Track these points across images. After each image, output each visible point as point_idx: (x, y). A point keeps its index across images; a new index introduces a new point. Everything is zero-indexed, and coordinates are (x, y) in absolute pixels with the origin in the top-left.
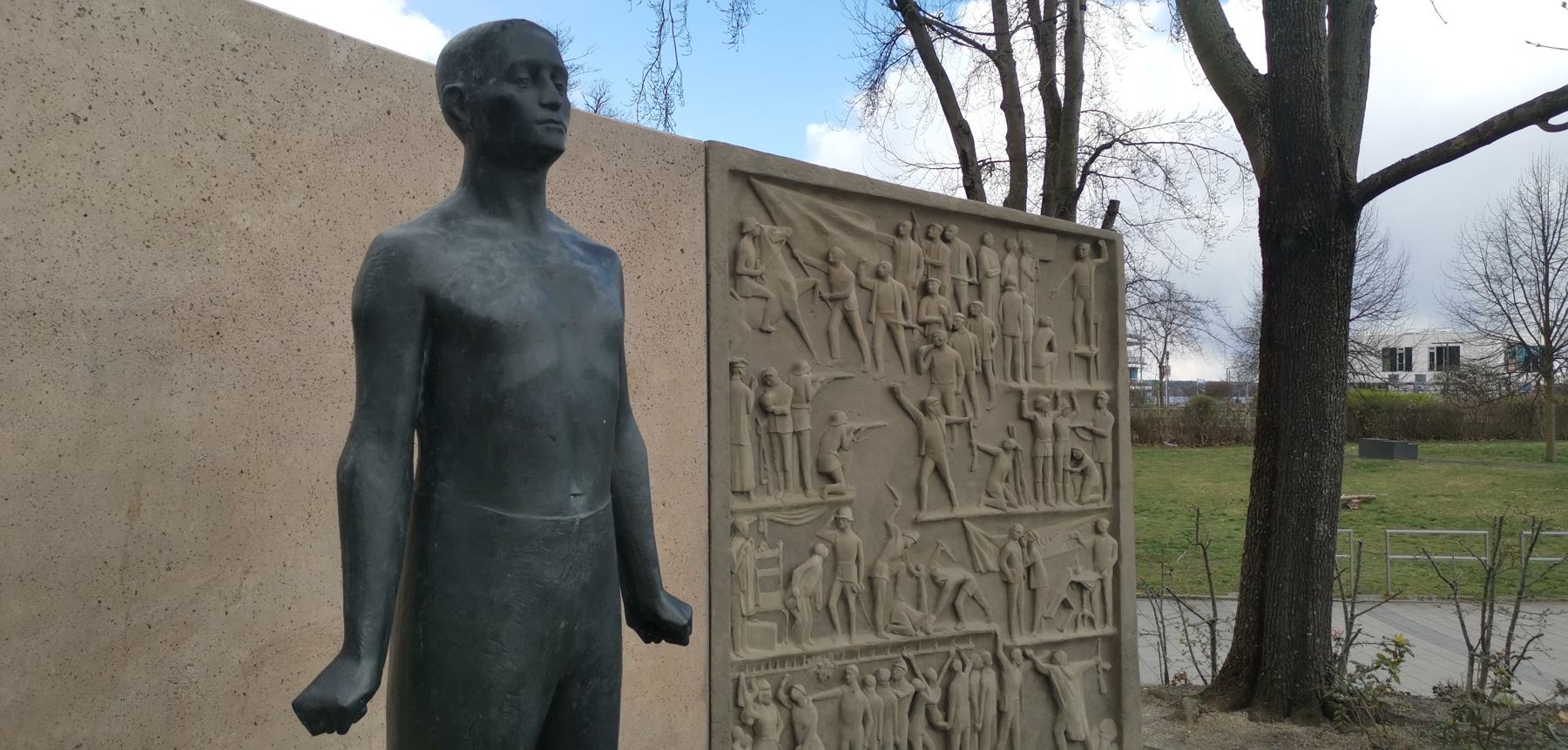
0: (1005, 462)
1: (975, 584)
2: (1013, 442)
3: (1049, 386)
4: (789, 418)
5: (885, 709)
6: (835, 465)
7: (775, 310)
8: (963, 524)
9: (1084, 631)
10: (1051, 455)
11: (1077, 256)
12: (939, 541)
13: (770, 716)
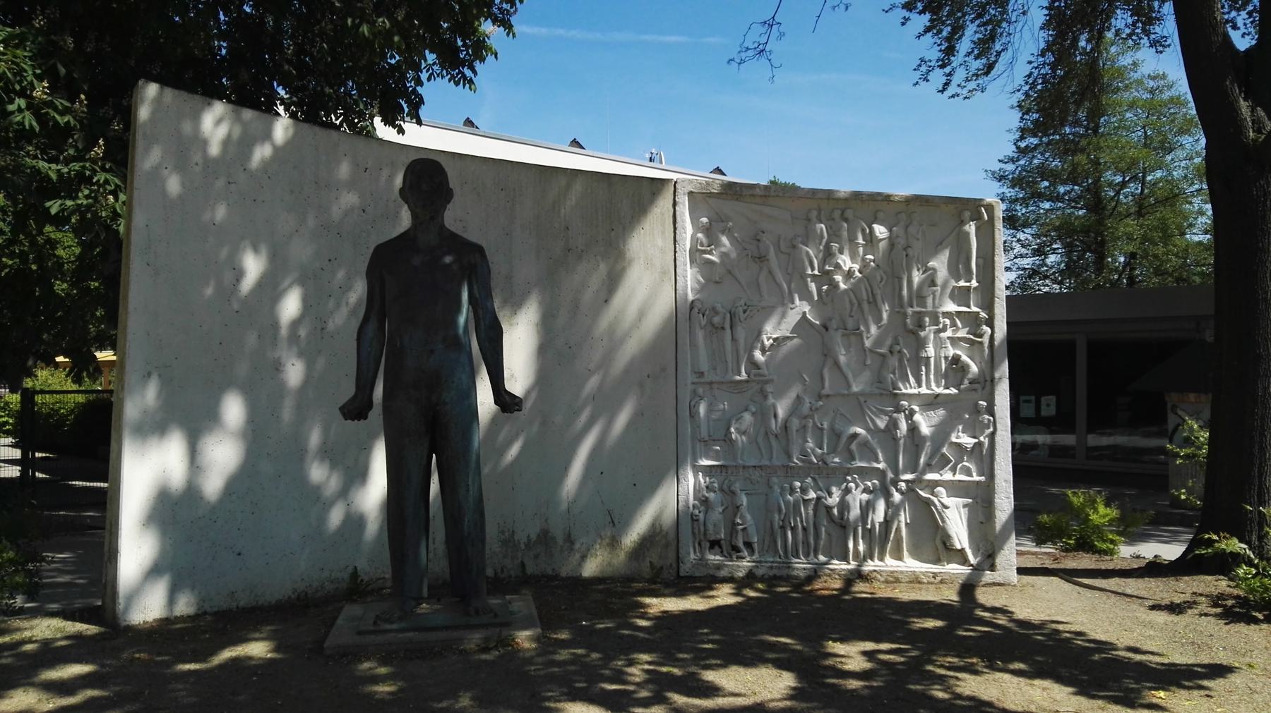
4: (728, 331)
5: (794, 505)
8: (858, 399)
10: (933, 355)
12: (840, 408)
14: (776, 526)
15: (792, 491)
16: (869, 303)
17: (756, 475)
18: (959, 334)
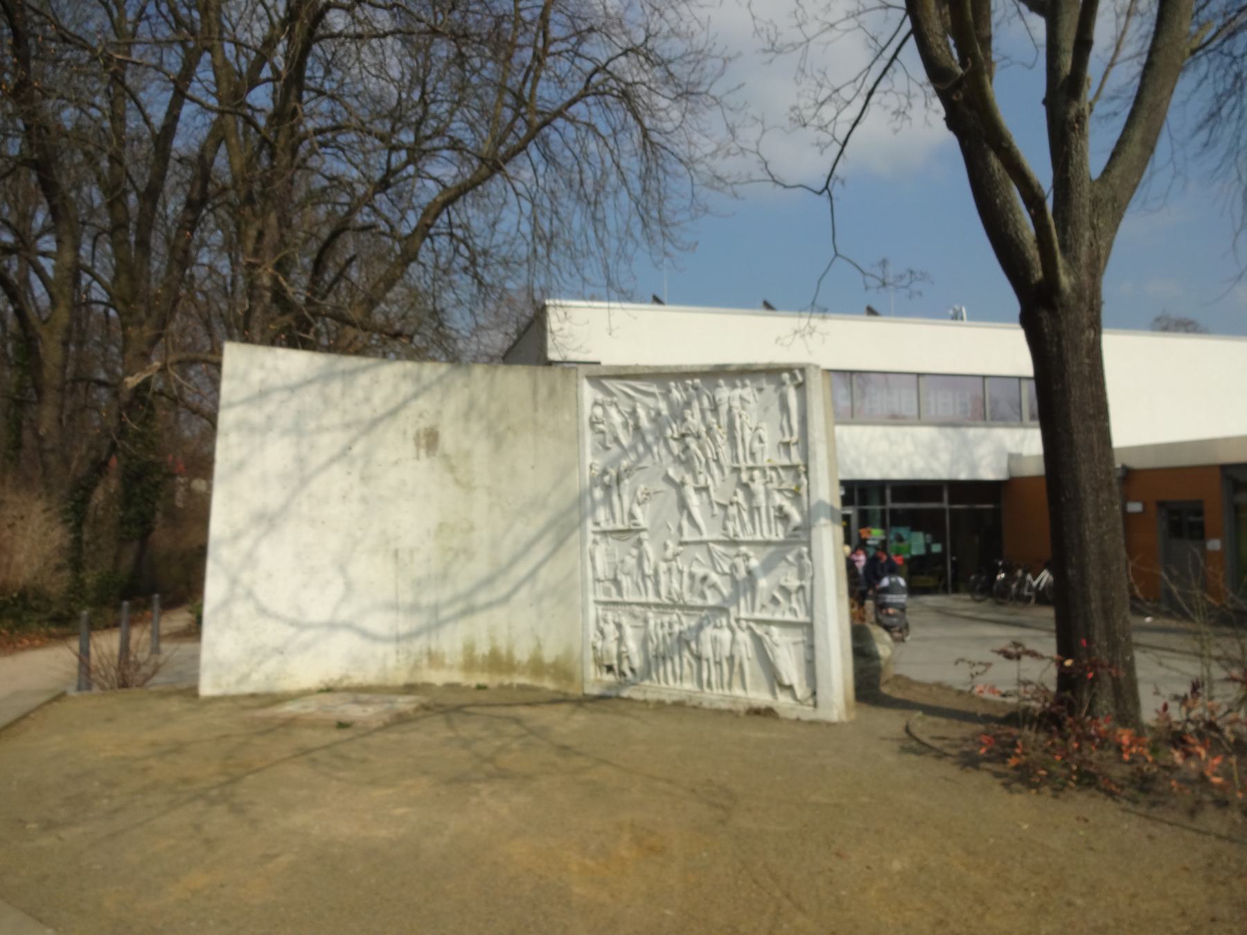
0: (733, 510)
1: (714, 577)
2: (735, 499)
3: (759, 464)
6: (638, 511)
7: (609, 437)
9: (789, 617)
11: (783, 384)
13: (610, 629)
14: (651, 657)
15: (662, 625)
16: (714, 460)
17: (637, 610)
18: (784, 486)
